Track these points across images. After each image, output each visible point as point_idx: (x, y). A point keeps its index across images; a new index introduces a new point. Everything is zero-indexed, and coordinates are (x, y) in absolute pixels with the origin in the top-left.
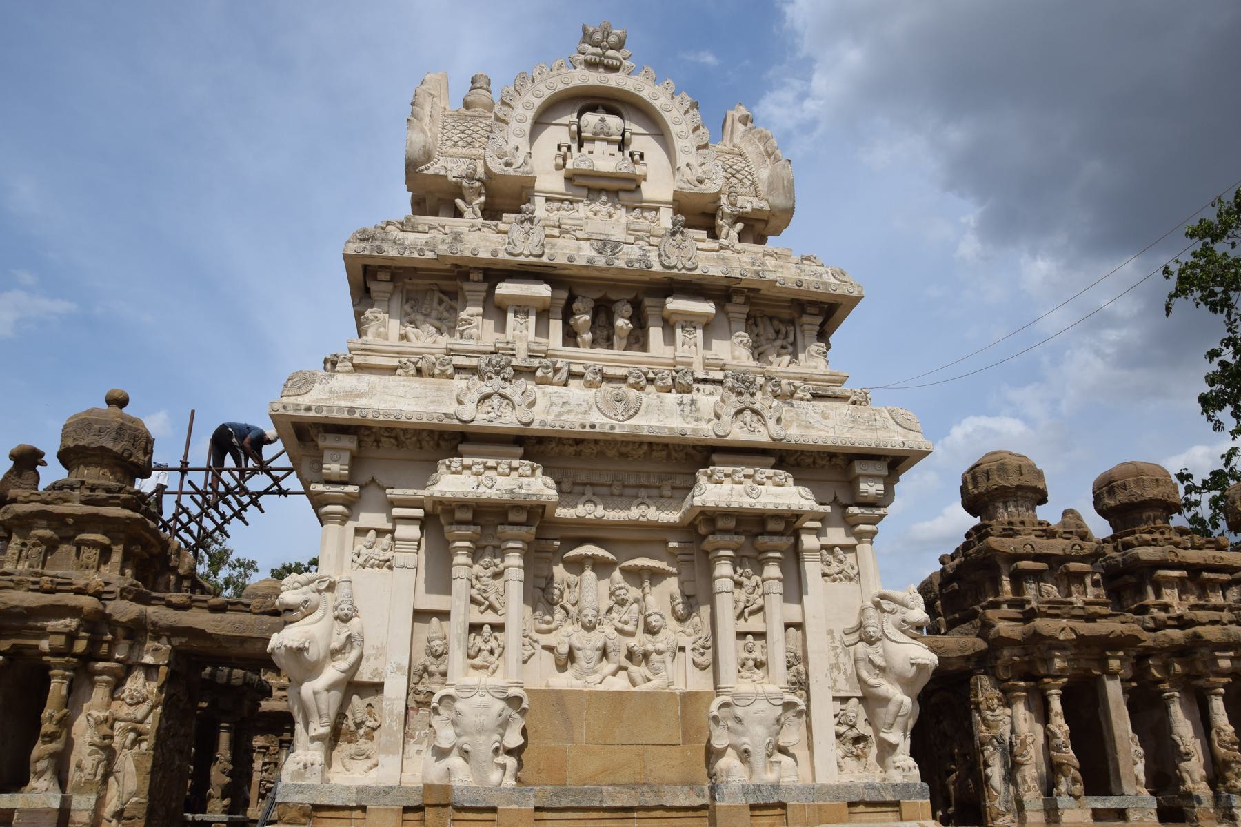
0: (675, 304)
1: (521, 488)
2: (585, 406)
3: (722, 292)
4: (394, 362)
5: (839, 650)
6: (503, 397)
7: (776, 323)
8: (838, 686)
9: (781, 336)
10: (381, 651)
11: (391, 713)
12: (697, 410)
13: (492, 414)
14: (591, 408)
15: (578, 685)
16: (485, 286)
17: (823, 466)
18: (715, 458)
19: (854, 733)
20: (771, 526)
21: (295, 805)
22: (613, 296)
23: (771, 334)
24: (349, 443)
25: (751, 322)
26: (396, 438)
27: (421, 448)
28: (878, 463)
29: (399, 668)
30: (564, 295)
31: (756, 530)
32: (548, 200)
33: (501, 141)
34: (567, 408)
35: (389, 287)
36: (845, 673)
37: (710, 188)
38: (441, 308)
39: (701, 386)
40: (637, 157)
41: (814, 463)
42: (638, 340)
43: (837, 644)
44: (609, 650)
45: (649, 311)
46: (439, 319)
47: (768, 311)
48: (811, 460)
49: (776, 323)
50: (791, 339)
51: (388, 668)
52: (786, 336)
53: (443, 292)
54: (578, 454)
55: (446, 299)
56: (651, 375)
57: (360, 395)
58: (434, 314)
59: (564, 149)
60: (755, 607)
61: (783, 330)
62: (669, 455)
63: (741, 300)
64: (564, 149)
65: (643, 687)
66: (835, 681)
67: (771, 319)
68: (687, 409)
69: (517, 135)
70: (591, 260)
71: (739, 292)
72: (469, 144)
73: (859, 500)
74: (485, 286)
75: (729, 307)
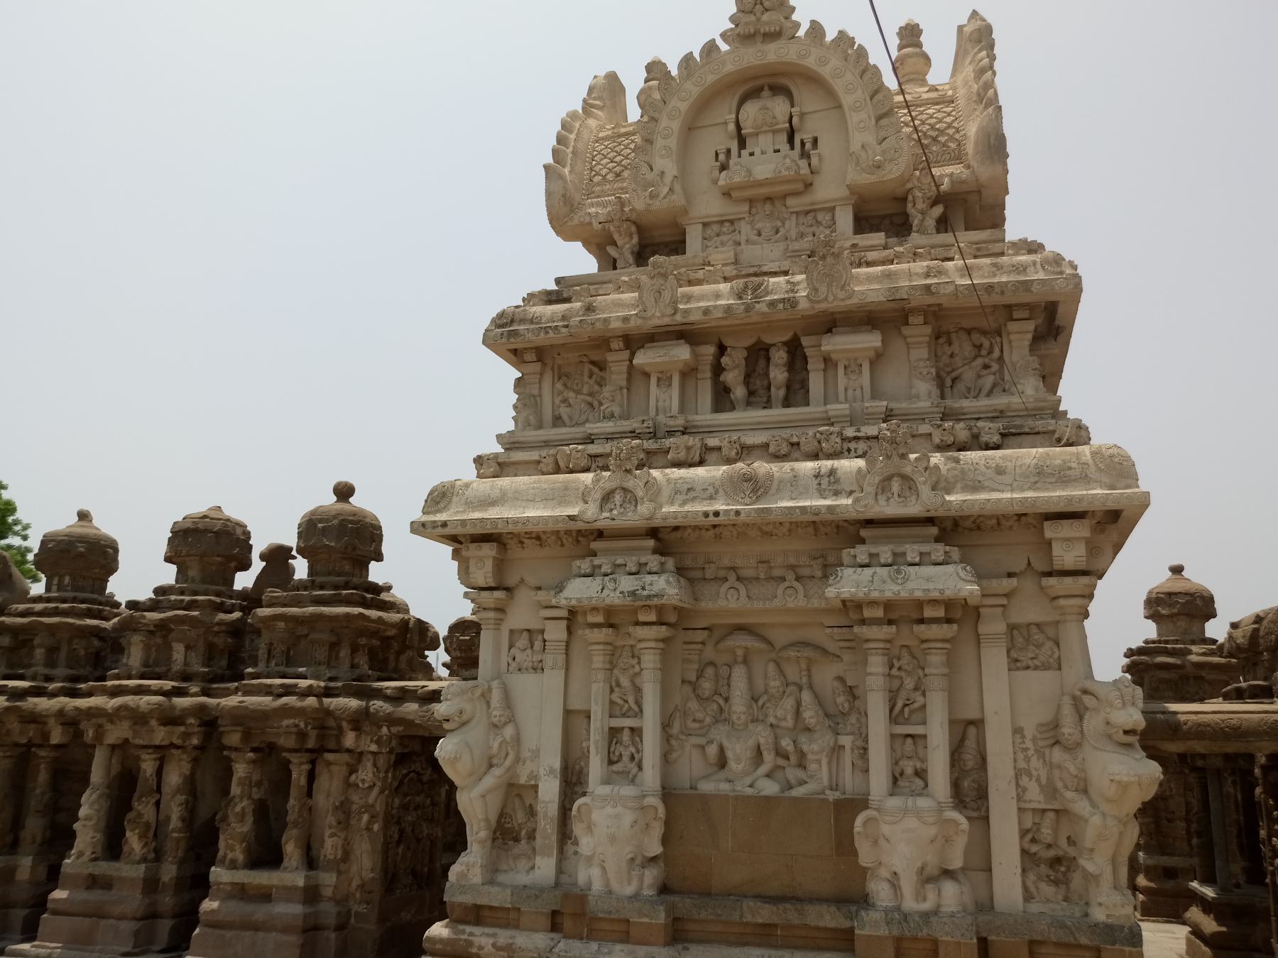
0: (837, 344)
1: (643, 588)
2: (711, 490)
3: (887, 319)
4: (533, 455)
5: (1030, 753)
6: (624, 489)
7: (975, 336)
8: (1028, 796)
9: (984, 352)
10: (536, 754)
11: (545, 815)
12: (837, 481)
13: (615, 512)
14: (717, 492)
15: (725, 787)
16: (626, 354)
17: (1011, 527)
18: (864, 533)
19: (1051, 853)
20: (929, 613)
21: (460, 905)
22: (768, 339)
23: (968, 350)
24: (489, 550)
25: (942, 340)
26: (538, 538)
27: (562, 545)
28: (1076, 523)
29: (552, 771)
30: (709, 350)
31: (915, 616)
32: (705, 225)
33: (645, 169)
34: (692, 494)
35: (537, 367)
36: (1038, 780)
37: (894, 172)
38: (592, 382)
39: (852, 445)
40: (808, 146)
41: (999, 524)
42: (796, 392)
43: (1029, 744)
45: (808, 352)
46: (591, 394)
47: (967, 324)
48: (994, 521)
49: (975, 336)
50: (996, 353)
51: (542, 772)
52: (991, 352)
53: (593, 363)
54: (718, 537)
55: (596, 370)
56: (795, 440)
57: (493, 503)
58: (585, 390)
59: (722, 157)
60: (916, 705)
61: (986, 344)
62: (816, 530)
63: (921, 319)
64: (722, 157)
65: (797, 792)
66: (1024, 790)
67: (969, 332)
68: (825, 481)
69: (662, 156)
70: (728, 309)
71: (914, 311)
72: (618, 175)
73: (1056, 567)
74: (626, 354)
75: (906, 331)
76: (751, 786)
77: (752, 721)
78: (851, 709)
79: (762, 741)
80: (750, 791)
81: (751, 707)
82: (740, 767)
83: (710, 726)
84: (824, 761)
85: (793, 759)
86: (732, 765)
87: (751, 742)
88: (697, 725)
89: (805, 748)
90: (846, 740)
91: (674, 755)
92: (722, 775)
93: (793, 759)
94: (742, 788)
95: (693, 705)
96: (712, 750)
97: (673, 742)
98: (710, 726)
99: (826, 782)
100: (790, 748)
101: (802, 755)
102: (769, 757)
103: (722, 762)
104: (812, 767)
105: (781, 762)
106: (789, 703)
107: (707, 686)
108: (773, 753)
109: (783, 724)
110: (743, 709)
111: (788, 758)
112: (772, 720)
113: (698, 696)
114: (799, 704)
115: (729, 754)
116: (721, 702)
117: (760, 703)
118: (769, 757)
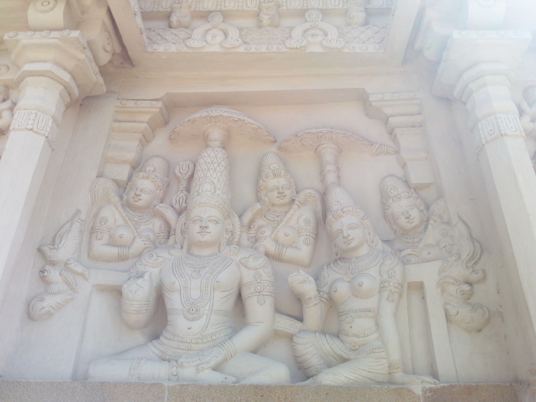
44: (244, 294)
76: (216, 369)
77: (229, 243)
78: (425, 222)
79: (248, 276)
80: (216, 378)
81: (228, 216)
82: (197, 326)
83: (140, 255)
84: (388, 309)
85: (313, 313)
86: (180, 323)
87: (227, 277)
88: (114, 251)
89: (342, 289)
90: (427, 273)
91: (49, 302)
92: (154, 348)
93: (313, 313)
94: (198, 371)
95: (112, 215)
96: (139, 293)
97: (54, 274)
98: (140, 255)
99: (395, 356)
100: (309, 288)
101: (332, 304)
102: (260, 311)
103: (158, 318)
104: (361, 325)
105: (286, 324)
106: (302, 217)
107: (146, 186)
108: (269, 302)
109: (289, 253)
110: (215, 213)
111: (300, 319)
112: (269, 245)
113: (128, 206)
114: (323, 218)
115: (174, 301)
116: (170, 215)
117: (247, 218)
118: (261, 313)
